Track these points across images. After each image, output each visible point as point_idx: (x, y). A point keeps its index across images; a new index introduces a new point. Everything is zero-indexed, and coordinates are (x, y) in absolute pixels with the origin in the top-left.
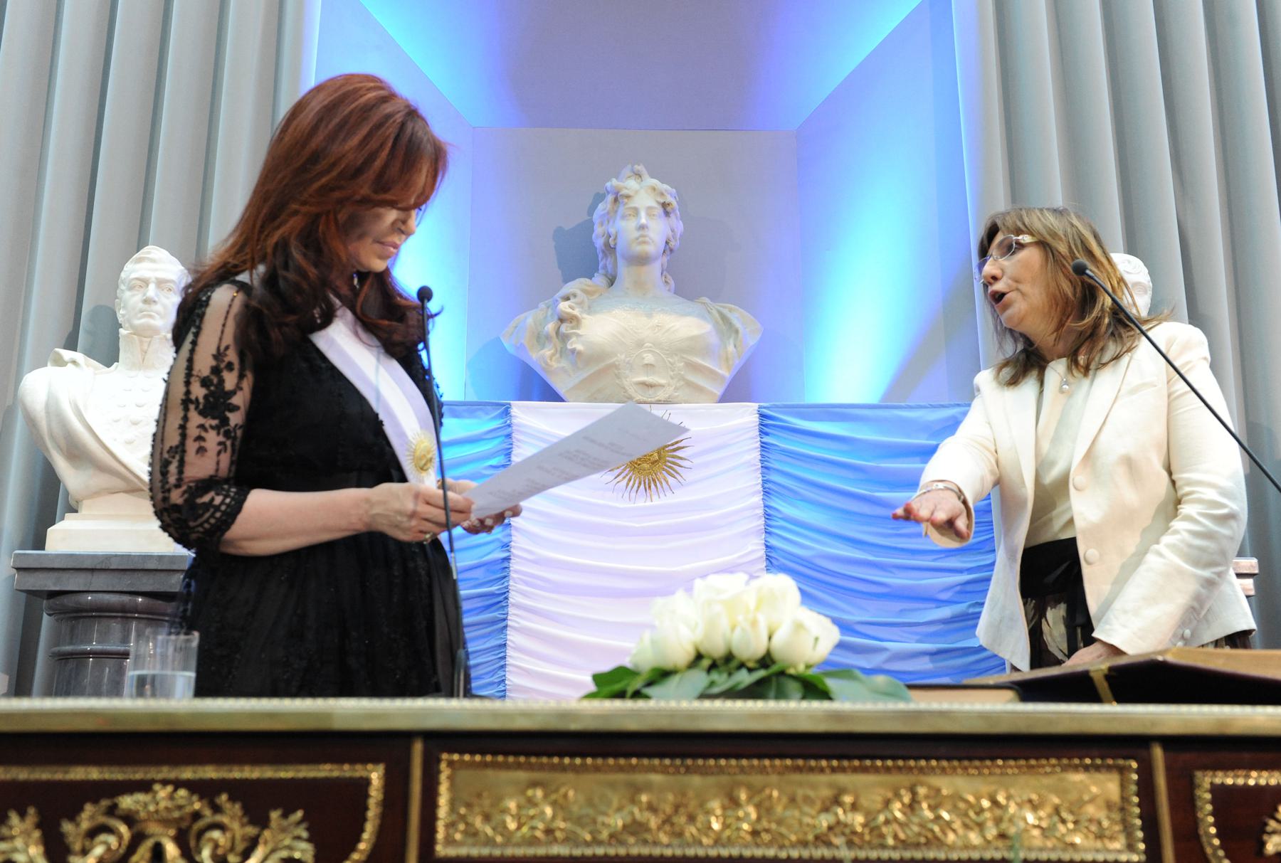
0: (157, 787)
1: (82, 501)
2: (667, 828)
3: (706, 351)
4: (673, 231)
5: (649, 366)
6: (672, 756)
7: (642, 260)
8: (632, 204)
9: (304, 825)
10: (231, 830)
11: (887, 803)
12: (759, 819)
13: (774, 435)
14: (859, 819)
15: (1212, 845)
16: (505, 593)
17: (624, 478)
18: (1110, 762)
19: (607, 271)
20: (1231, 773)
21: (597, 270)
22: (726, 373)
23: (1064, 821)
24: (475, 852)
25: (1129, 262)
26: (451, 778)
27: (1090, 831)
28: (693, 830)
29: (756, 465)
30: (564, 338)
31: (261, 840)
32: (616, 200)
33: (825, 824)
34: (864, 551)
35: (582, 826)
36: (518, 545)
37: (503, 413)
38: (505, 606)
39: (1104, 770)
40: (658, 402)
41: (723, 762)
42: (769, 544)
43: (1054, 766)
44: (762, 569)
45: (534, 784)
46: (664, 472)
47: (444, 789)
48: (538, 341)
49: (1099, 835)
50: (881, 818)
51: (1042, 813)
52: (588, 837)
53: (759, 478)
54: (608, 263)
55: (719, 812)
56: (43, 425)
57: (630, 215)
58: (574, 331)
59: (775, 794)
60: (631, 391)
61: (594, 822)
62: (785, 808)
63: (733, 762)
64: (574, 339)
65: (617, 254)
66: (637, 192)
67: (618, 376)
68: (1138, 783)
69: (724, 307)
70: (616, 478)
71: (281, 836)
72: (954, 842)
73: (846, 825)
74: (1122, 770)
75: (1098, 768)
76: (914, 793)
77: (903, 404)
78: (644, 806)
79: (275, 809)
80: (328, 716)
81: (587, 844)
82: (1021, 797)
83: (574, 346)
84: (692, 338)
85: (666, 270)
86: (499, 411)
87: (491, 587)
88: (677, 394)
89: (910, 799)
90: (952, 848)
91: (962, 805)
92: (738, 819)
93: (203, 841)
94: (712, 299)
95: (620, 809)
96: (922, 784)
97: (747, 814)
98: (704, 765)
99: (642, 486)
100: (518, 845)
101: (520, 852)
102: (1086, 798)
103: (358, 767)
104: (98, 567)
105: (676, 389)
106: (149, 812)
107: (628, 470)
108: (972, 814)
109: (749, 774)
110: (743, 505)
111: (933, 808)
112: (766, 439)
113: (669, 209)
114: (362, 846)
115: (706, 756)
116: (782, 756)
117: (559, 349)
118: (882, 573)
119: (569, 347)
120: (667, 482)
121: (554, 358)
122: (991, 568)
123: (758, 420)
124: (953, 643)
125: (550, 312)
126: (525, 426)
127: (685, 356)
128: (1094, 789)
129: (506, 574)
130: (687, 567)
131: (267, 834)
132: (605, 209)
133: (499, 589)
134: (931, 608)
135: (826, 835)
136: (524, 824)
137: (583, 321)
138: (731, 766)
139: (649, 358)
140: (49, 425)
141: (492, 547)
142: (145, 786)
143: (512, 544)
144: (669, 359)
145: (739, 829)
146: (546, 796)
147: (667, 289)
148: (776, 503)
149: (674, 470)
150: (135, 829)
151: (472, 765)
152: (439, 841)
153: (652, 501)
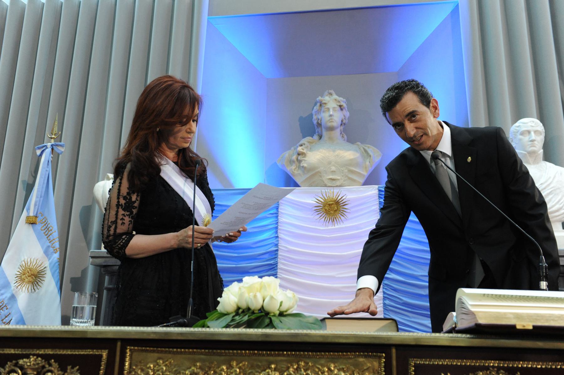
0: (31, 357)
3: (357, 165)
4: (344, 116)
5: (333, 172)
7: (331, 129)
9: (79, 372)
10: (54, 373)
11: (288, 368)
16: (276, 264)
17: (323, 217)
18: (375, 354)
21: (315, 133)
22: (366, 174)
25: (533, 122)
26: (131, 356)
30: (300, 161)
32: (321, 105)
34: (422, 245)
36: (281, 245)
40: (337, 186)
43: (353, 355)
45: (160, 358)
46: (339, 214)
48: (290, 163)
53: (378, 216)
54: (319, 130)
55: (225, 370)
57: (326, 111)
64: (303, 162)
65: (323, 127)
66: (329, 102)
68: (385, 362)
70: (320, 217)
76: (298, 365)
78: (198, 367)
79: (69, 365)
83: (303, 165)
84: (351, 160)
87: (271, 261)
88: (345, 183)
89: (296, 367)
94: (361, 143)
97: (236, 371)
99: (331, 220)
102: (365, 368)
103: (100, 351)
106: (28, 366)
109: (237, 356)
113: (342, 107)
117: (298, 166)
119: (301, 165)
120: (340, 218)
121: (296, 170)
123: (378, 192)
125: (295, 151)
127: (347, 167)
130: (345, 253)
132: (316, 109)
137: (307, 154)
139: (333, 168)
141: (270, 246)
142: (27, 356)
143: (279, 244)
144: (342, 169)
146: (163, 363)
147: (343, 139)
150: (23, 372)
151: (138, 350)
153: (335, 226)
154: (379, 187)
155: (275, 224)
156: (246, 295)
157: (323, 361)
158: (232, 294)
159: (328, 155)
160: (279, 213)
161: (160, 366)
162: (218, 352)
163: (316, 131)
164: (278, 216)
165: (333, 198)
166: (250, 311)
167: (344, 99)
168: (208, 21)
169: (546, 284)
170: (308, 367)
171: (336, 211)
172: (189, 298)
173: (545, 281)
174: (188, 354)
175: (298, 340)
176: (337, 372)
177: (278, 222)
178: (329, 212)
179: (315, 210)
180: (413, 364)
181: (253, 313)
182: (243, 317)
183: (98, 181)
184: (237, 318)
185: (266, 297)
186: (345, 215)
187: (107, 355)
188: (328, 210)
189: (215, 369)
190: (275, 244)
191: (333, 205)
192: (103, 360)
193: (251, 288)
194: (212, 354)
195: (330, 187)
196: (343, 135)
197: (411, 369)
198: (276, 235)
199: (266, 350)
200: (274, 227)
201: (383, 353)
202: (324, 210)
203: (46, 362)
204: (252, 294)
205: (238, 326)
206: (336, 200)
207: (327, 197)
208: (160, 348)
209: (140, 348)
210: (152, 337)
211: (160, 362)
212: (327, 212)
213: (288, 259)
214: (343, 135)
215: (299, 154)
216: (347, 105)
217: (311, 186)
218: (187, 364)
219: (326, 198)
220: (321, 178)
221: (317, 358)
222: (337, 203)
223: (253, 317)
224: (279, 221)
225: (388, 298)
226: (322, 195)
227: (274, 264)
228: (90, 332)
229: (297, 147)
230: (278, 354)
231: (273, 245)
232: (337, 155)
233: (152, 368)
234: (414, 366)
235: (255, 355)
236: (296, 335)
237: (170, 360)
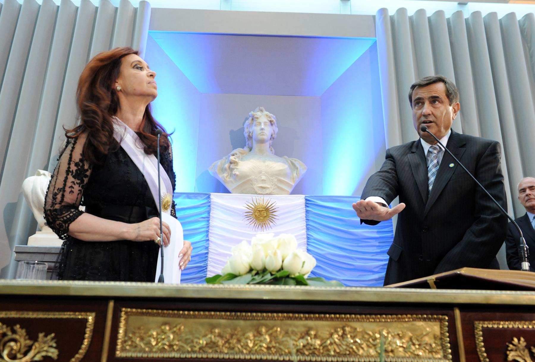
1: (43, 227)
2: (227, 345)
3: (286, 175)
4: (274, 131)
5: (263, 181)
6: (231, 311)
7: (262, 141)
8: (259, 121)
9: (55, 340)
10: (20, 342)
11: (331, 335)
12: (271, 341)
13: (312, 207)
14: (318, 342)
15: (483, 356)
16: (206, 266)
17: (253, 223)
18: (435, 316)
19: (249, 146)
20: (491, 323)
21: (245, 146)
22: (293, 184)
23: (414, 344)
24: (134, 355)
27: (426, 349)
28: (239, 346)
29: (303, 218)
30: (232, 170)
31: (34, 347)
32: (253, 119)
33: (302, 344)
35: (187, 344)
36: (211, 248)
37: (207, 197)
38: (206, 271)
39: (432, 320)
40: (267, 194)
41: (254, 314)
42: (308, 249)
43: (409, 318)
45: (165, 324)
46: (268, 221)
47: (122, 324)
48: (222, 171)
49: (430, 351)
50: (329, 342)
51: (404, 341)
52: (189, 349)
53: (305, 223)
54: (249, 143)
55: (252, 338)
56: (30, 197)
57: (258, 125)
59: (279, 329)
61: (192, 342)
62: (283, 337)
63: (259, 314)
64: (235, 170)
66: (260, 116)
67: (252, 184)
68: (448, 327)
69: (292, 159)
71: (43, 346)
72: (362, 354)
73: (311, 345)
74: (441, 320)
75: (429, 319)
76: (344, 331)
78: (217, 334)
79: (41, 332)
80: (68, 288)
81: (188, 352)
82: (394, 333)
83: (235, 173)
84: (280, 170)
85: (272, 146)
86: (206, 197)
88: (274, 191)
90: (361, 356)
91: (366, 336)
92: (261, 341)
93: (6, 347)
95: (205, 336)
96: (348, 326)
97: (265, 339)
98: (245, 316)
99: (260, 226)
100: (156, 352)
101: (156, 355)
102: (424, 333)
104: (47, 252)
105: (274, 189)
108: (371, 340)
109: (267, 320)
111: (353, 337)
112: (308, 209)
113: (272, 123)
114: (81, 351)
115: (246, 311)
116: (282, 312)
117: (230, 174)
118: (352, 261)
119: (233, 173)
120: (269, 225)
121: (228, 177)
123: (304, 201)
125: (227, 160)
126: (216, 202)
127: (277, 177)
128: (428, 329)
129: (206, 259)
131: (37, 344)
132: (248, 123)
133: (203, 265)
134: (371, 275)
135: (302, 349)
136: (160, 342)
137: (239, 163)
138: (258, 316)
139: (264, 177)
140: (32, 198)
143: (209, 247)
144: (272, 178)
145: (261, 346)
146: (170, 329)
147: (272, 152)
149: (272, 220)
152: (118, 349)
153: (263, 231)
155: (206, 228)
160: (211, 217)
161: (165, 333)
162: (243, 316)
163: (246, 145)
164: (209, 220)
165: (263, 205)
167: (274, 115)
168: (148, 34)
170: (355, 334)
173: (527, 262)
174: (204, 318)
176: (391, 339)
177: (209, 226)
178: (259, 218)
179: (246, 216)
183: (26, 177)
186: (274, 221)
189: (239, 336)
190: (205, 247)
192: (88, 326)
194: (235, 318)
195: (260, 194)
196: (271, 148)
198: (207, 239)
200: (203, 231)
202: (254, 215)
203: (9, 328)
204: (270, 252)
206: (266, 207)
207: (257, 204)
208: (167, 310)
209: (139, 310)
211: (165, 328)
212: (257, 218)
213: (217, 261)
214: (271, 148)
215: (231, 163)
216: (276, 121)
217: (242, 192)
218: (203, 331)
219: (257, 205)
220: (251, 186)
221: (366, 321)
222: (267, 209)
224: (210, 225)
226: (253, 202)
227: (204, 267)
228: (74, 288)
229: (229, 156)
230: (319, 317)
232: (267, 166)
233: (155, 336)
234: (482, 331)
237: (178, 327)
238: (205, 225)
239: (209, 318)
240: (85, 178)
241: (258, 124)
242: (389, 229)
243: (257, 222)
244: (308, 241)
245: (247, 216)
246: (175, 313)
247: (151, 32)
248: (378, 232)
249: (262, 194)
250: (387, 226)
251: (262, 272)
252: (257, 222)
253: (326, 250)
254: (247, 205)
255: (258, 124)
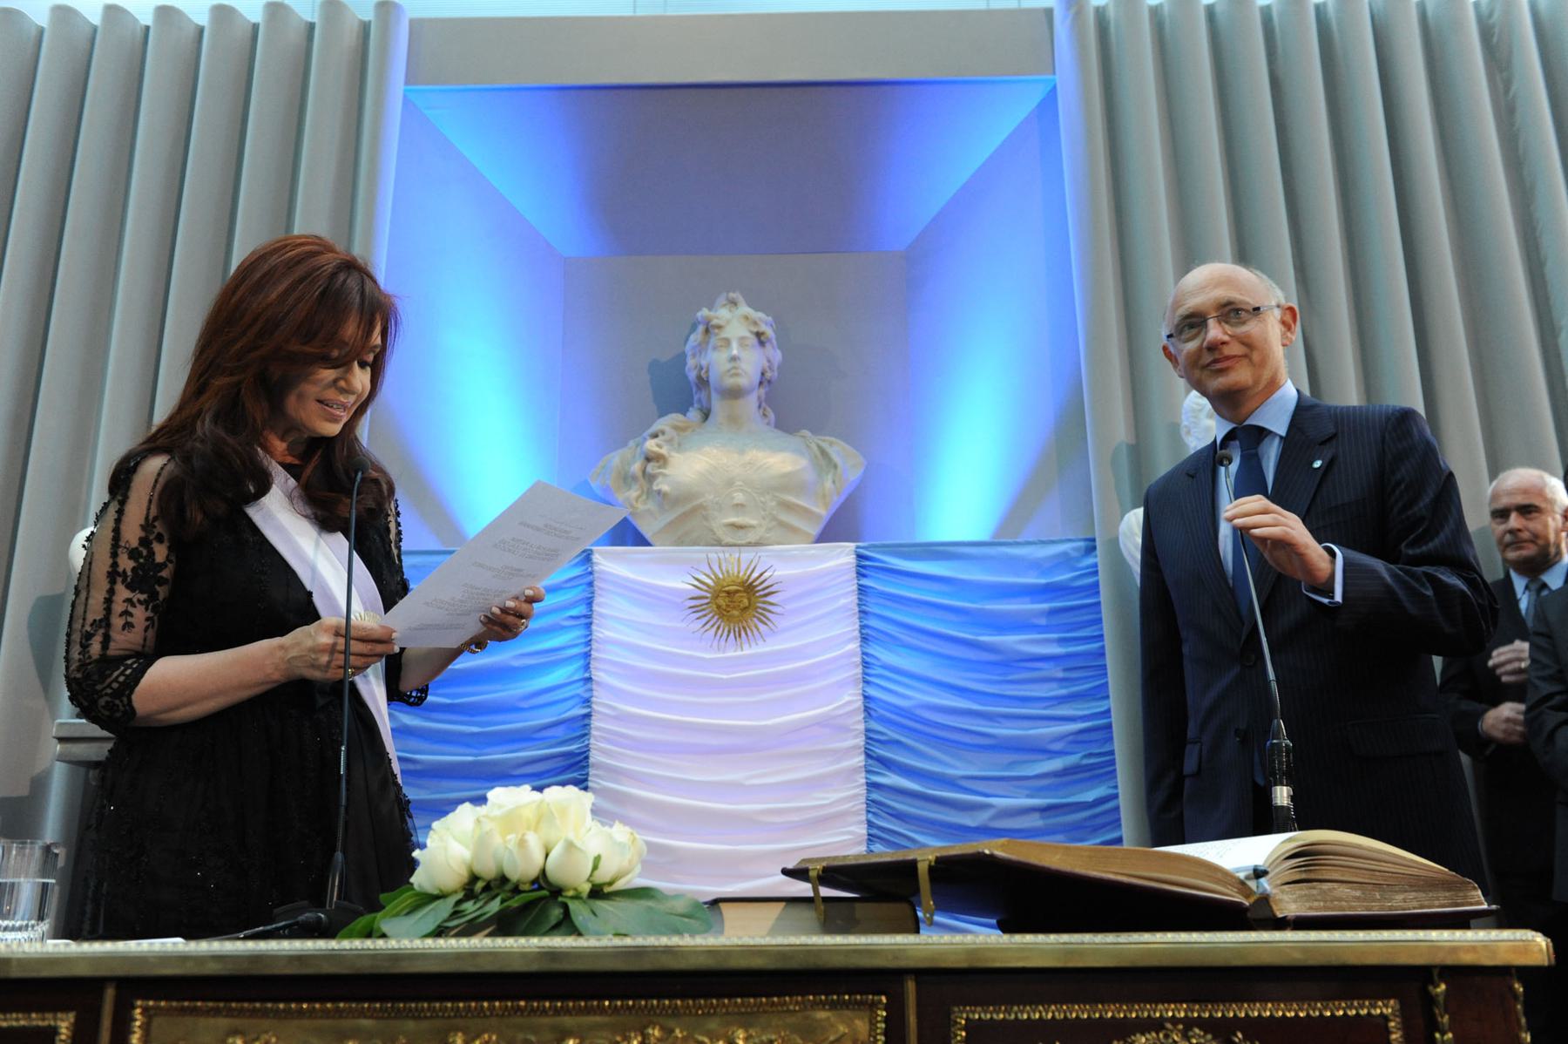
3: (801, 488)
4: (769, 361)
7: (735, 393)
8: (724, 334)
13: (879, 578)
17: (713, 626)
18: (858, 997)
19: (702, 406)
21: (692, 405)
22: (823, 512)
26: (146, 1028)
30: (651, 478)
32: (707, 331)
34: (969, 699)
40: (749, 544)
42: (866, 694)
44: (859, 721)
46: (755, 619)
53: (855, 624)
57: (721, 346)
58: (661, 470)
60: (720, 533)
64: (660, 479)
66: (728, 322)
67: (706, 518)
68: (886, 1020)
69: (821, 440)
75: (846, 1005)
77: (1010, 540)
83: (659, 487)
94: (815, 431)
96: (654, 1025)
99: (732, 634)
103: (49, 1015)
107: (716, 617)
109: (466, 1016)
110: (839, 652)
112: (865, 582)
113: (762, 338)
117: (645, 489)
119: (655, 488)
120: (758, 630)
121: (640, 499)
122: (1108, 715)
123: (854, 561)
124: (1065, 797)
127: (777, 494)
128: (842, 1029)
129: (586, 731)
132: (695, 341)
133: (579, 748)
137: (670, 459)
139: (739, 497)
143: (594, 699)
144: (762, 499)
147: (766, 421)
148: (876, 651)
149: (765, 616)
151: (168, 1012)
153: (742, 650)
154: (858, 547)
155: (582, 646)
156: (497, 840)
157: (713, 1024)
158: (455, 838)
159: (725, 461)
160: (594, 616)
163: (695, 402)
164: (591, 623)
165: (738, 576)
166: (508, 887)
167: (768, 315)
169: (1288, 791)
171: (746, 609)
172: (335, 851)
174: (321, 1018)
175: (646, 965)
178: (728, 612)
180: (963, 1022)
181: (516, 890)
182: (486, 903)
184: (469, 906)
185: (553, 848)
186: (769, 620)
187: (72, 1028)
188: (724, 607)
190: (582, 700)
191: (738, 595)
193: (510, 820)
194: (393, 1015)
197: (956, 1035)
198: (587, 675)
199: (552, 998)
200: (576, 655)
201: (880, 993)
204: (512, 838)
205: (470, 930)
206: (747, 580)
207: (723, 574)
208: (238, 1001)
209: (174, 1004)
210: (212, 969)
214: (765, 409)
217: (679, 542)
219: (721, 576)
220: (705, 523)
222: (749, 588)
223: (515, 903)
224: (594, 637)
225: (879, 838)
226: (711, 568)
228: (19, 960)
229: (645, 439)
231: (576, 700)
232: (750, 463)
234: (965, 1028)
235: (519, 1013)
236: (639, 952)
238: (578, 638)
239: (333, 1018)
240: (160, 585)
241: (723, 344)
242: (1095, 631)
243: (722, 624)
244: (865, 673)
245: (696, 609)
246: (254, 1007)
247: (410, 91)
248: (1061, 641)
249: (735, 545)
250: (1088, 621)
251: (498, 882)
252: (722, 624)
253: (915, 697)
254: (694, 577)
255: (723, 344)
